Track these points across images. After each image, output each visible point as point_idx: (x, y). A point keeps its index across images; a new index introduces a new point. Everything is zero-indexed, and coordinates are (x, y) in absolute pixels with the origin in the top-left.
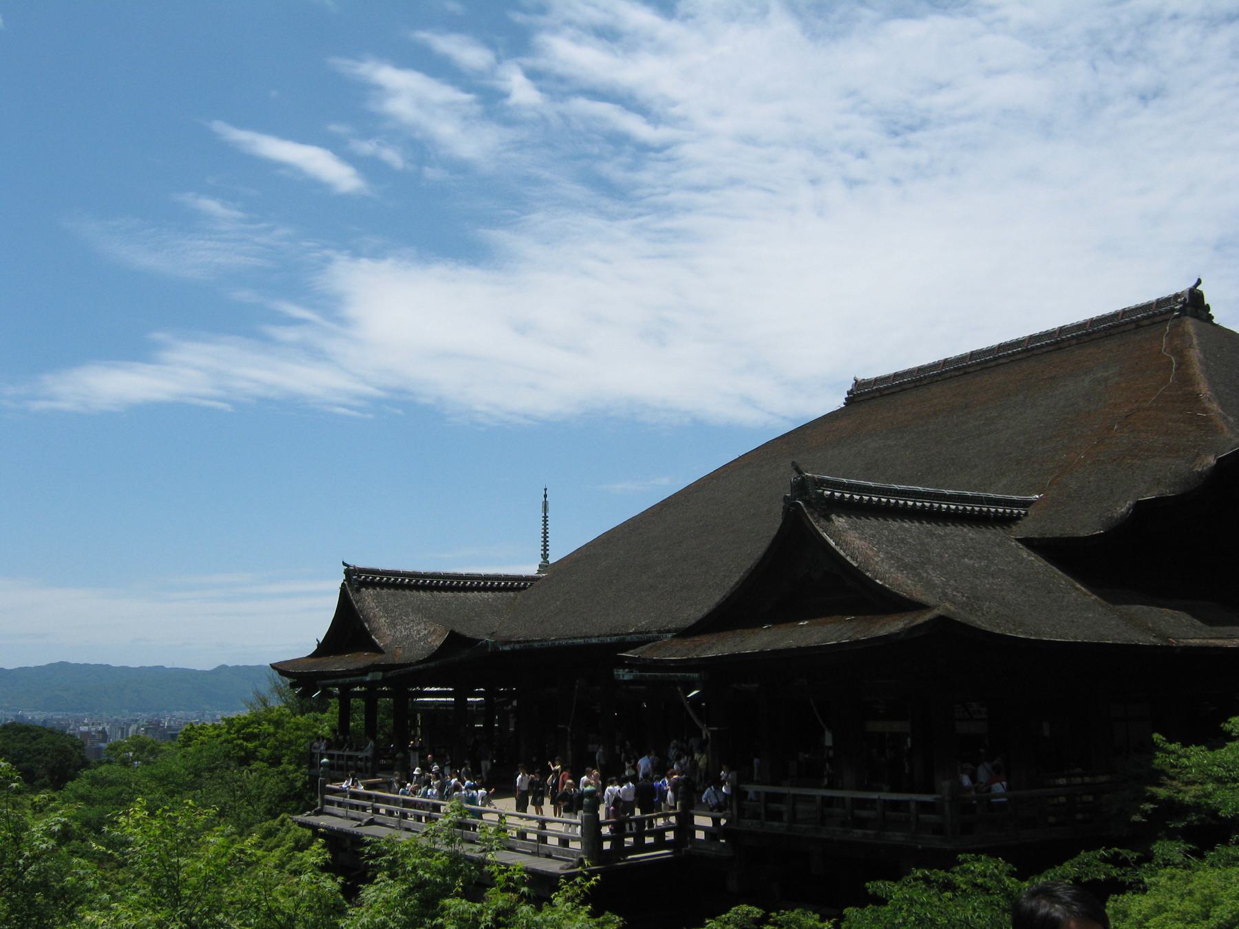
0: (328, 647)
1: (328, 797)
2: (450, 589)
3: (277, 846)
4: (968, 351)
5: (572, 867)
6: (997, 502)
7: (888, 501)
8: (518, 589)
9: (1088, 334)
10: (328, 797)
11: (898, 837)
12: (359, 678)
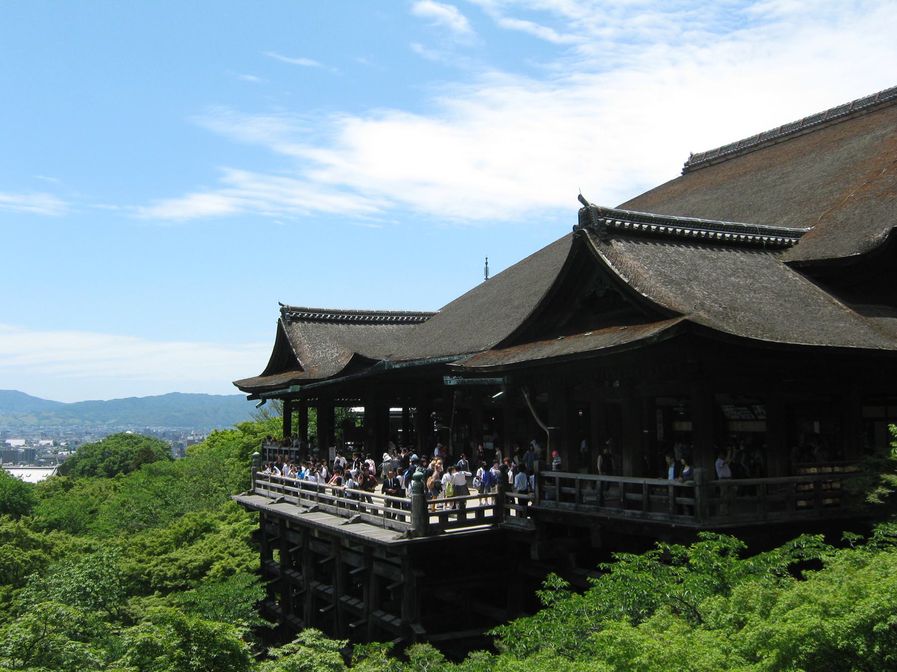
1: (258, 481)
3: (237, 520)
4: (779, 126)
5: (402, 538)
6: (771, 232)
7: (666, 229)
8: (418, 322)
9: (876, 105)
10: (258, 481)
11: (658, 517)
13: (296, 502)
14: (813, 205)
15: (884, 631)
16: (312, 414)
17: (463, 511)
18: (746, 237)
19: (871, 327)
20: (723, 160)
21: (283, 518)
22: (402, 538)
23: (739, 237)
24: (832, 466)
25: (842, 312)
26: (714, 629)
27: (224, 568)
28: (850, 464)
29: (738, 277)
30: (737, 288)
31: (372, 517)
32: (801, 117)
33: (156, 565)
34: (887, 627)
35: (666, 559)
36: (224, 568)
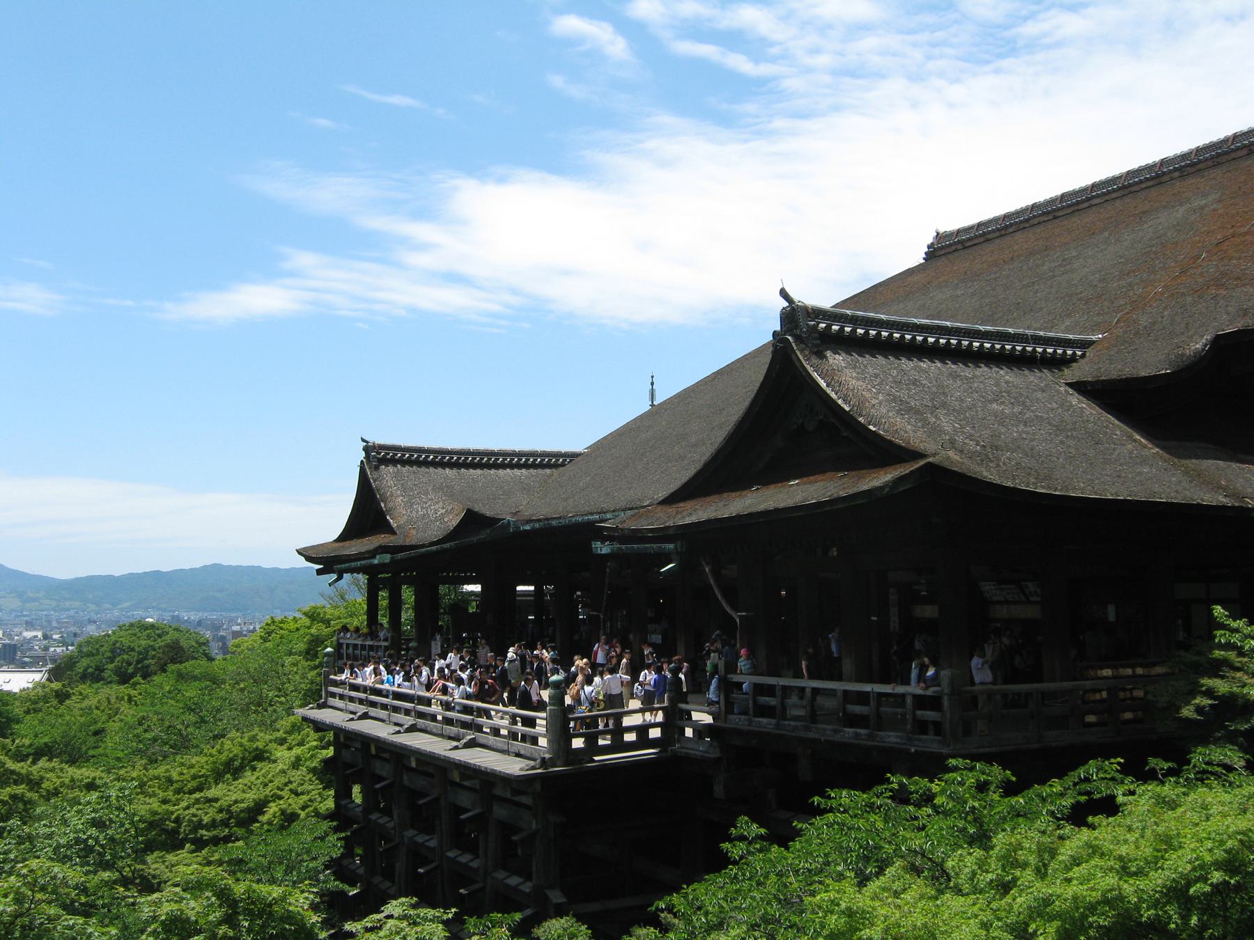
0: (353, 530)
2: (480, 466)
3: (301, 744)
4: (1059, 193)
5: (533, 768)
6: (1047, 341)
7: (902, 337)
8: (556, 466)
9: (1193, 165)
11: (892, 738)
13: (385, 717)
14: (1106, 303)
15: (1204, 894)
16: (408, 594)
17: (619, 731)
18: (1014, 348)
19: (1186, 473)
20: (981, 240)
21: (366, 741)
22: (533, 768)
23: (1003, 347)
24: (1133, 667)
25: (1145, 452)
26: (968, 894)
27: (283, 812)
28: (1155, 664)
29: (1003, 403)
30: (1001, 419)
31: (492, 740)
32: (1090, 182)
33: (188, 808)
34: (1208, 889)
35: (902, 797)
36: (283, 812)
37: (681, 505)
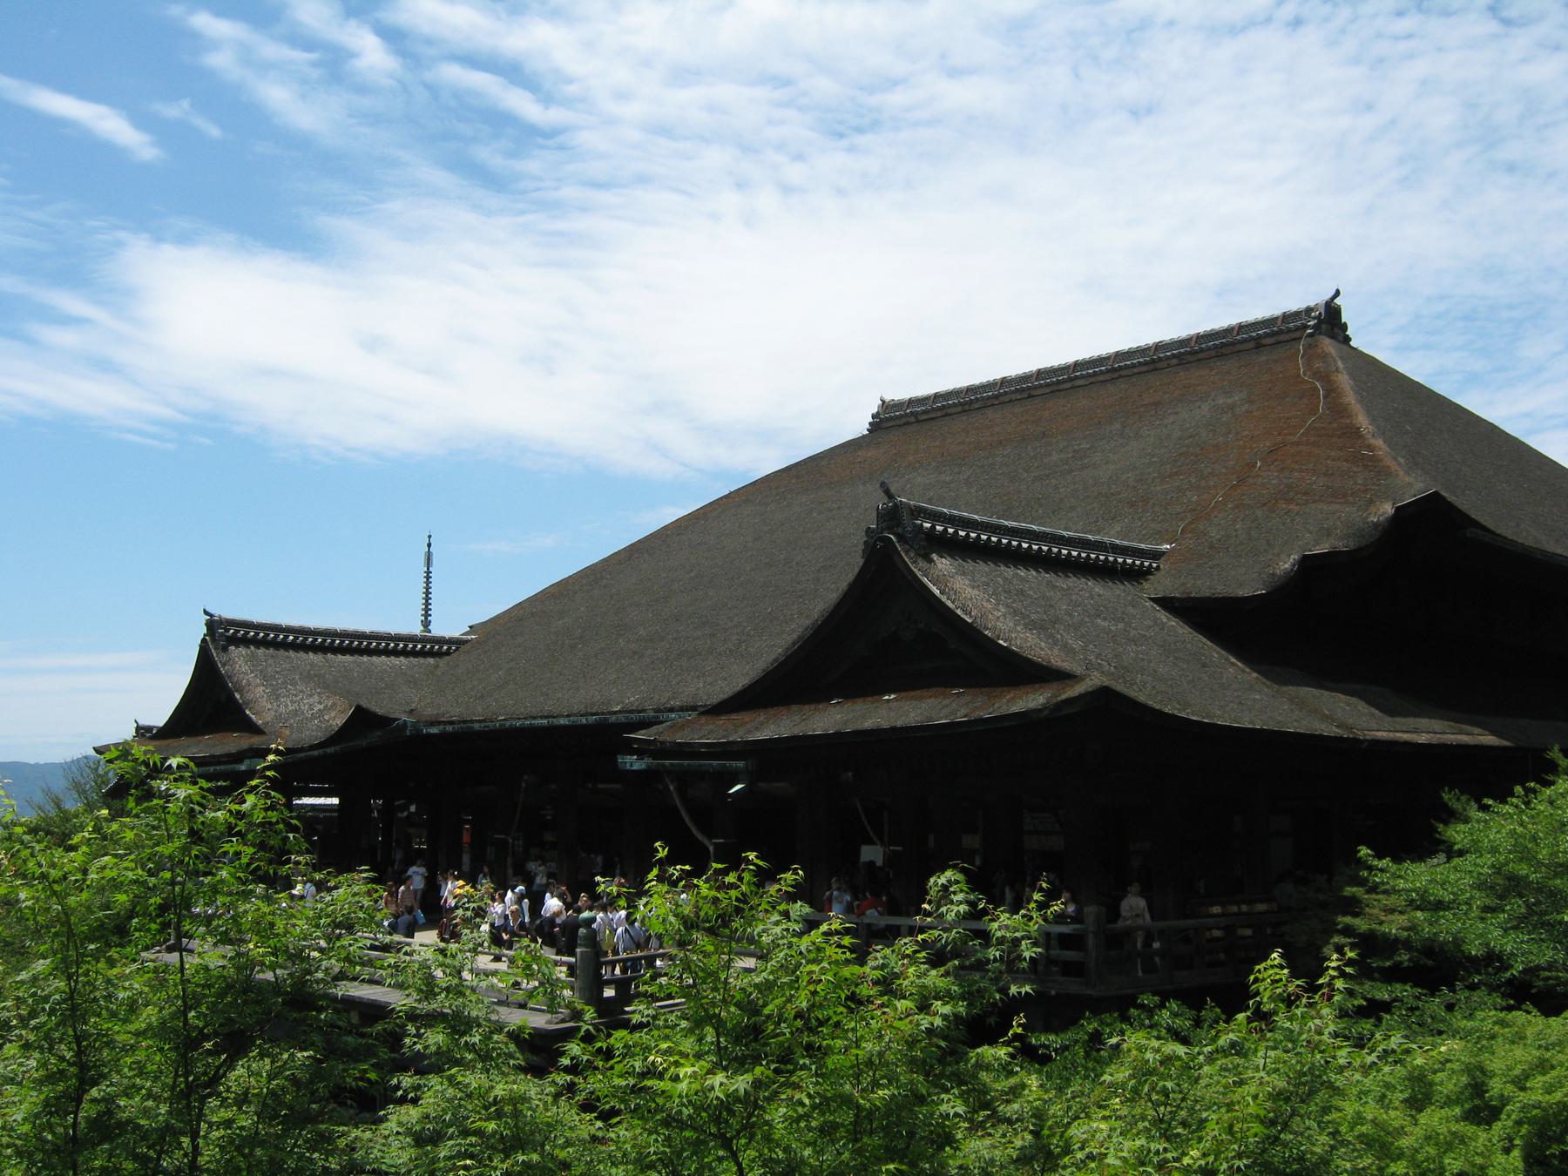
5: (563, 1021)
6: (1124, 551)
8: (440, 654)
12: (230, 767)
19: (1291, 700)
24: (1238, 904)
29: (1105, 619)
37: (734, 716)
